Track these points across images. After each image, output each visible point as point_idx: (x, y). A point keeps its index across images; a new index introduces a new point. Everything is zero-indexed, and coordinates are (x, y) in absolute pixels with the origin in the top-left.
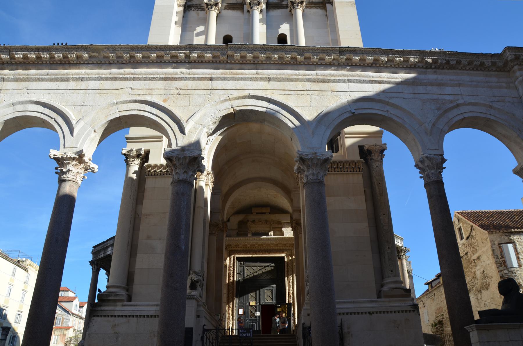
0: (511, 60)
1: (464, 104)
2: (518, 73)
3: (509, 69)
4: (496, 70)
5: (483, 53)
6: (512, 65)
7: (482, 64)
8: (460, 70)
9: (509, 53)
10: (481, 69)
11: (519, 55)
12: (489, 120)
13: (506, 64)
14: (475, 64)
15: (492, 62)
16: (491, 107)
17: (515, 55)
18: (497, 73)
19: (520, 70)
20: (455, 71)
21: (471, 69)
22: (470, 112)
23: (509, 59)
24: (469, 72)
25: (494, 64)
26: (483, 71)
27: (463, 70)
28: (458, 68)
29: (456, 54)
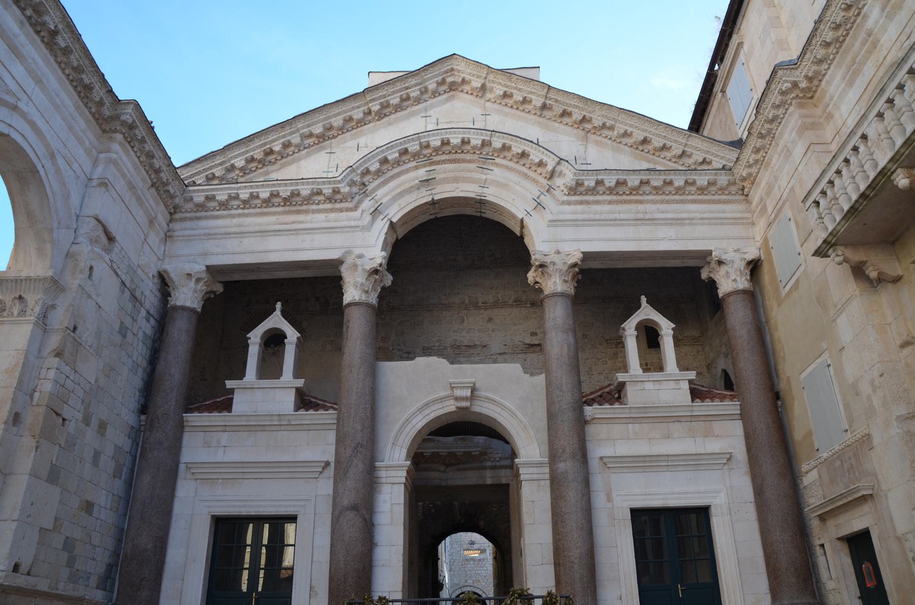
0: (124, 123)
1: (24, 116)
2: (116, 147)
3: (107, 129)
4: (93, 115)
5: (106, 77)
6: (118, 128)
7: (89, 88)
8: (56, 61)
9: (130, 111)
10: (80, 92)
11: (137, 126)
12: (34, 171)
13: (115, 118)
14: (83, 76)
15: (101, 99)
16: (52, 156)
17: (134, 121)
18: (91, 118)
19: (120, 144)
20: (49, 55)
21: (71, 77)
22: (23, 135)
23: (123, 118)
24: (64, 77)
25: (101, 103)
26: (79, 96)
27: (60, 67)
28: (56, 56)
29: (77, 37)
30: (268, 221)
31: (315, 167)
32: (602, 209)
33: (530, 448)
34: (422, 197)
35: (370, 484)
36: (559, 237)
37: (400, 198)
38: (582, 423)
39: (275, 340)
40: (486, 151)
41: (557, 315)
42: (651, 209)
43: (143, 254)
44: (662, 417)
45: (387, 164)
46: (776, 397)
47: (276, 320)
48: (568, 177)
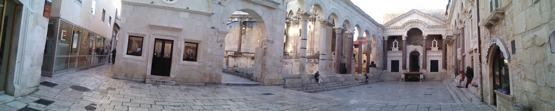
30: (394, 30)
31: (399, 24)
32: (430, 29)
33: (421, 54)
34: (410, 28)
35: (406, 58)
36: (425, 33)
37: (408, 28)
38: (426, 52)
39: (396, 43)
40: (418, 22)
41: (424, 41)
42: (436, 29)
43: (381, 35)
44: (435, 52)
45: (407, 24)
46: (446, 50)
47: (396, 41)
48: (427, 26)
